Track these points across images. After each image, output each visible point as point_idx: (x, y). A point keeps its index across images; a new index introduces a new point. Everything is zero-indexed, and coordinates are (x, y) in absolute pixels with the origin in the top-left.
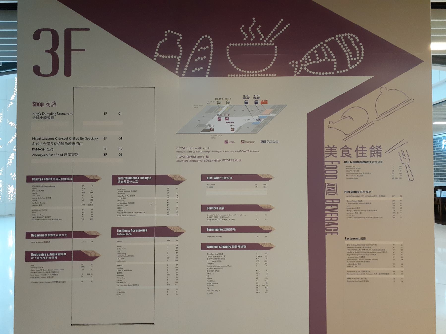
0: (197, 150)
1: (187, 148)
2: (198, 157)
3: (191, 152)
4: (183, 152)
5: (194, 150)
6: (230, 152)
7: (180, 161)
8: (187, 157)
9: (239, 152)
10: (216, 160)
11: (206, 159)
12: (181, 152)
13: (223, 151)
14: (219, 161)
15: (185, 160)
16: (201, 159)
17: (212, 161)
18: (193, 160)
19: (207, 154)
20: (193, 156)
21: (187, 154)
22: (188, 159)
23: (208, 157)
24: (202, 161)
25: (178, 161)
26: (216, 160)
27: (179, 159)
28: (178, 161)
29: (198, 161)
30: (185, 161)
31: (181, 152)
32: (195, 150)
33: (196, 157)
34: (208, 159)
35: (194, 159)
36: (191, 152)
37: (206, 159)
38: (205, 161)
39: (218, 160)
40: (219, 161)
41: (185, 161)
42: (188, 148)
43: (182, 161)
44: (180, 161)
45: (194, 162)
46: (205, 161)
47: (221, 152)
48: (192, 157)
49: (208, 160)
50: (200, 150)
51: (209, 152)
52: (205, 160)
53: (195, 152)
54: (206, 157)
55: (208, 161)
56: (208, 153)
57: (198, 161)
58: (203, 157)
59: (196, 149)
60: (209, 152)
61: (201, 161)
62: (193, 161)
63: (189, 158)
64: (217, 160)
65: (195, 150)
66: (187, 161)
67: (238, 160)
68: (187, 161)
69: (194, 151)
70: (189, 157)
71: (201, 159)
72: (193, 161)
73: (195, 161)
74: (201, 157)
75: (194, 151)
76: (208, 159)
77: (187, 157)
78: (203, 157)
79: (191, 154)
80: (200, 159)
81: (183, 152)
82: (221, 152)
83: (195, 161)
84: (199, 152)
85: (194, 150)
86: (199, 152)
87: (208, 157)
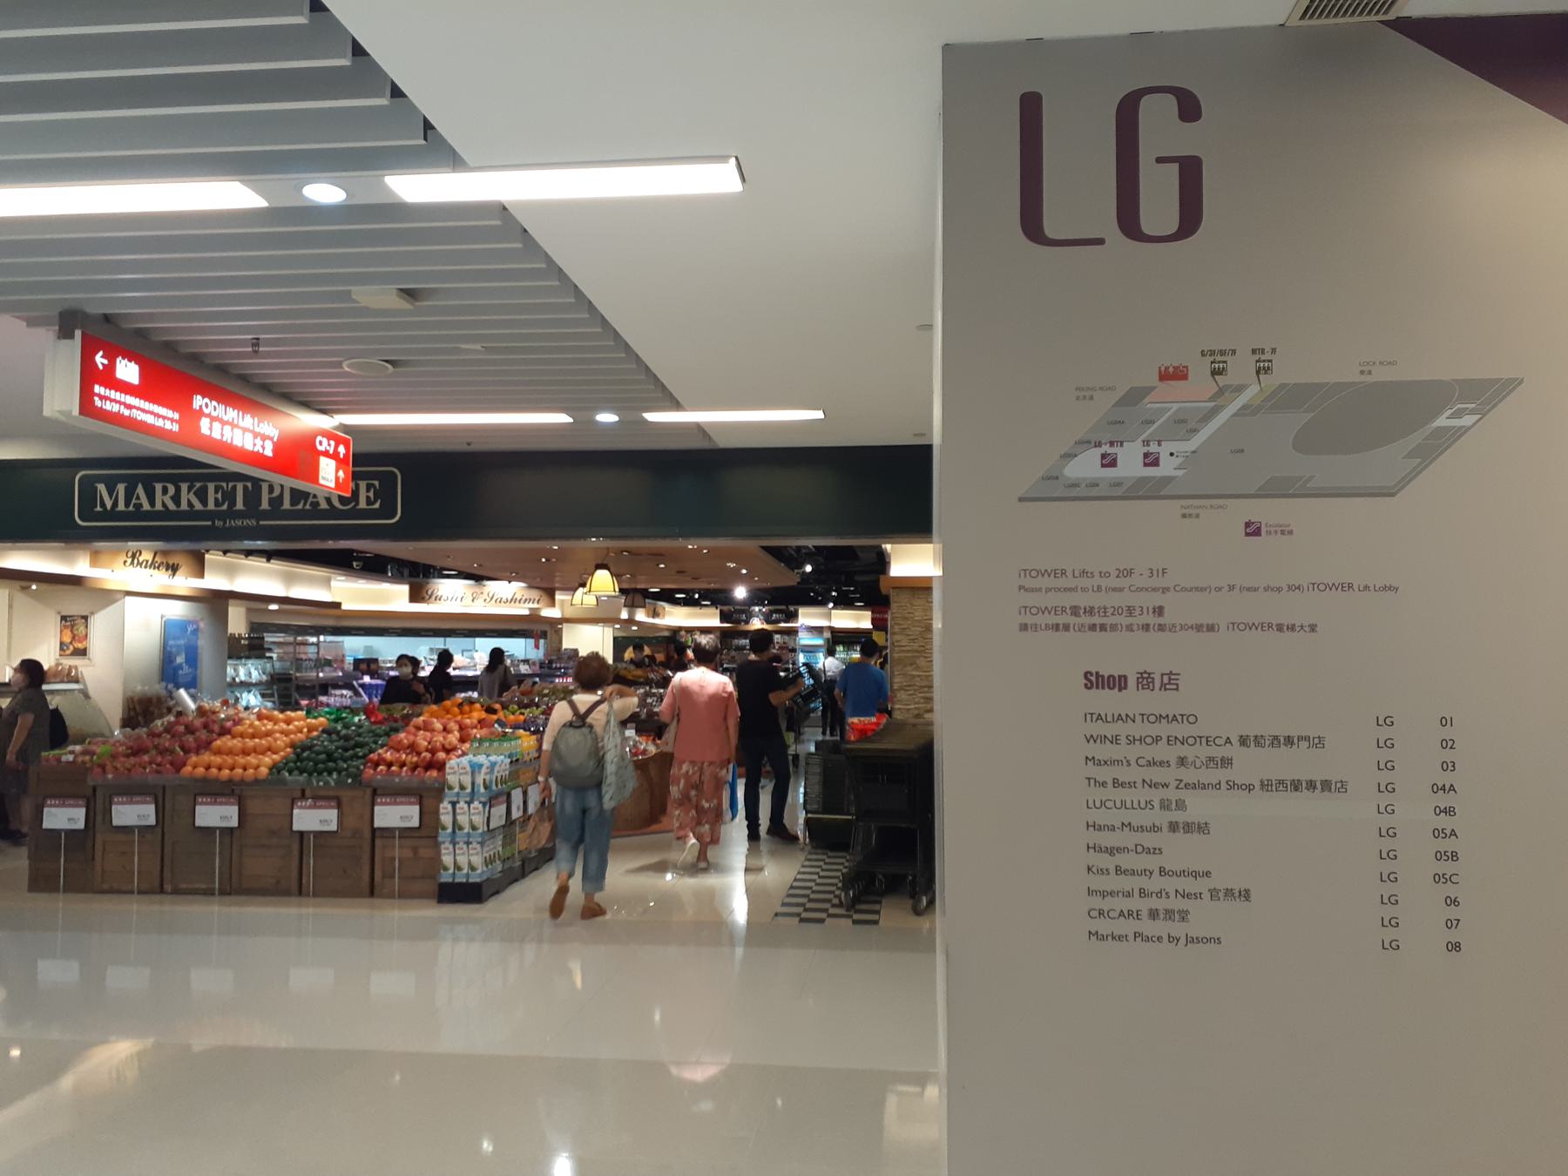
0: (1114, 582)
1: (1064, 573)
2: (1117, 611)
3: (1084, 590)
4: (1048, 590)
5: (1097, 581)
6: (1266, 589)
7: (1035, 627)
8: (1064, 610)
9: (1306, 588)
10: (1199, 628)
11: (1152, 620)
12: (1040, 590)
13: (1232, 588)
14: (1211, 628)
15: (1058, 625)
16: (1130, 620)
17: (1178, 628)
18: (1094, 625)
19: (1157, 599)
20: (1092, 608)
21: (1068, 600)
22: (1072, 620)
23: (1159, 611)
24: (1135, 628)
25: (1024, 627)
26: (1199, 628)
27: (1029, 620)
28: (1024, 627)
29: (1114, 627)
30: (1056, 627)
31: (1040, 590)
32: (1104, 583)
33: (1105, 612)
34: (1162, 623)
35: (1097, 620)
36: (1084, 590)
37: (1152, 620)
38: (1146, 627)
39: (1208, 625)
40: (1211, 628)
41: (1056, 627)
42: (1069, 574)
43: (1043, 627)
44: (1035, 627)
45: (1098, 634)
46: (1146, 627)
47: (1220, 589)
48: (1090, 611)
49: (1160, 625)
50: (1124, 582)
51: (1165, 590)
52: (1148, 625)
53: (1103, 588)
54: (1151, 611)
55: (1161, 628)
56: (1163, 592)
57: (1114, 627)
58: (1138, 611)
59: (1106, 575)
60: (1165, 590)
61: (1130, 628)
62: (1093, 627)
63: (1075, 615)
64: (1202, 625)
65: (1104, 583)
66: (1066, 628)
67: (1302, 627)
68: (1066, 628)
69: (1099, 588)
70: (1075, 611)
71: (1130, 620)
72: (1093, 627)
73: (1103, 628)
74: (1130, 611)
75: (1099, 588)
76: (1161, 620)
77: (1064, 610)
78: (1138, 611)
79: (1082, 600)
80: (1124, 620)
81: (1048, 590)
82: (1220, 589)
83: (1103, 628)
84: (1121, 590)
85: (1097, 581)
86: (1121, 590)
87: (1159, 611)
